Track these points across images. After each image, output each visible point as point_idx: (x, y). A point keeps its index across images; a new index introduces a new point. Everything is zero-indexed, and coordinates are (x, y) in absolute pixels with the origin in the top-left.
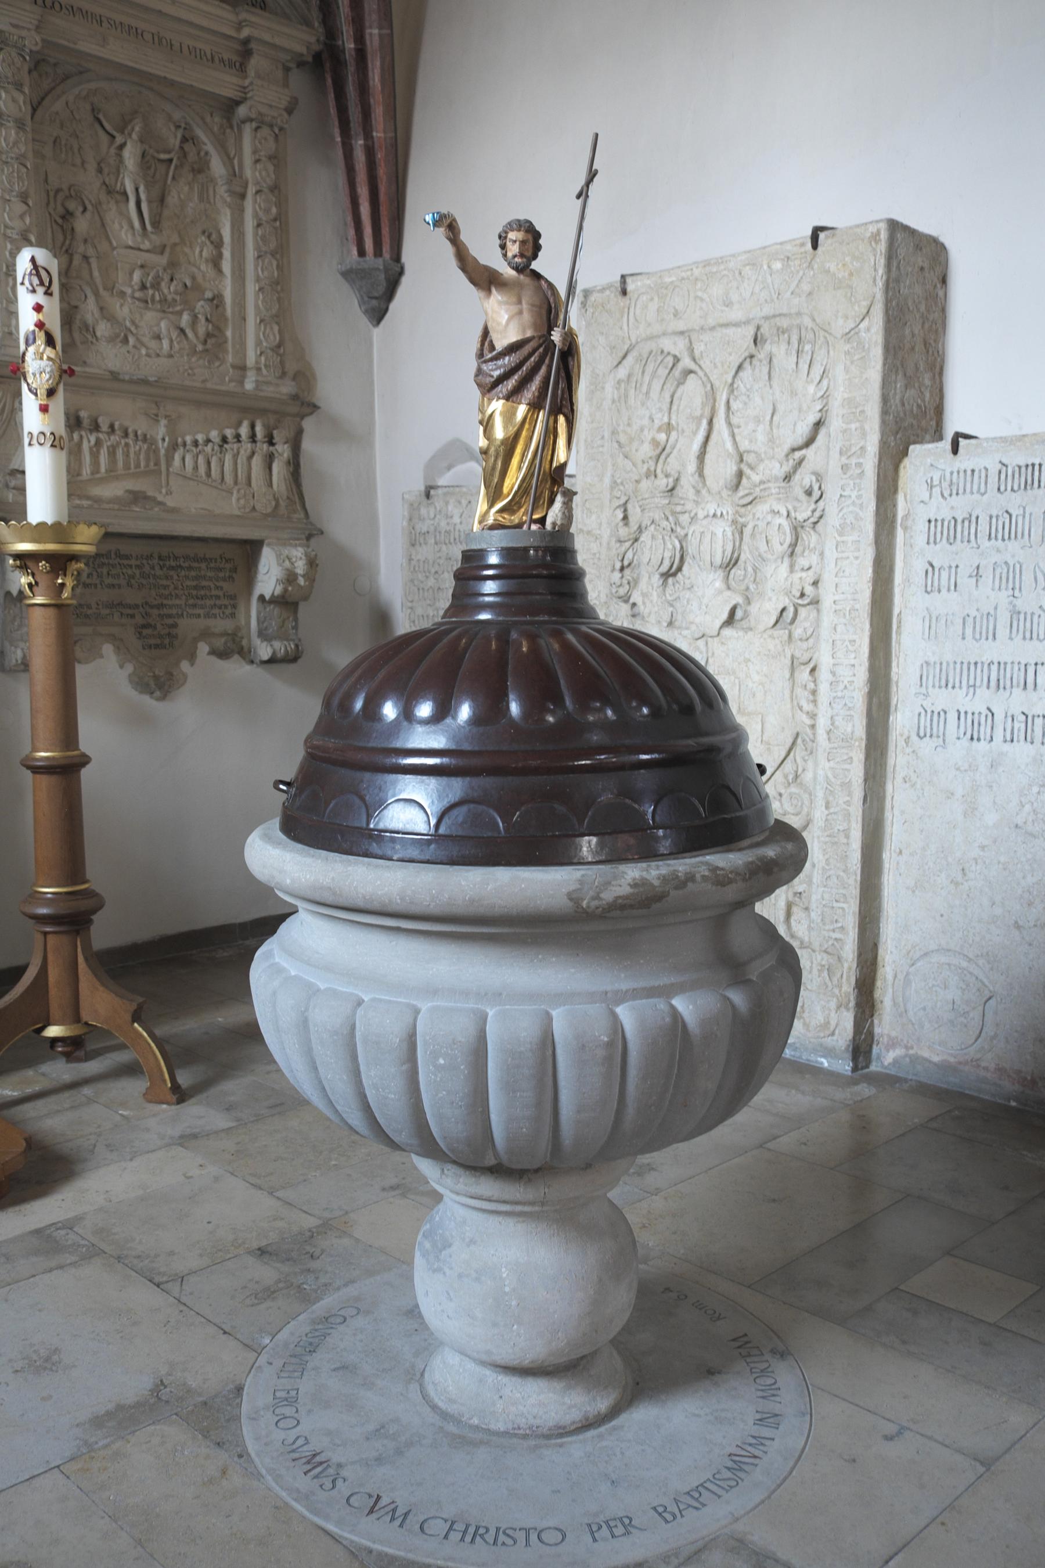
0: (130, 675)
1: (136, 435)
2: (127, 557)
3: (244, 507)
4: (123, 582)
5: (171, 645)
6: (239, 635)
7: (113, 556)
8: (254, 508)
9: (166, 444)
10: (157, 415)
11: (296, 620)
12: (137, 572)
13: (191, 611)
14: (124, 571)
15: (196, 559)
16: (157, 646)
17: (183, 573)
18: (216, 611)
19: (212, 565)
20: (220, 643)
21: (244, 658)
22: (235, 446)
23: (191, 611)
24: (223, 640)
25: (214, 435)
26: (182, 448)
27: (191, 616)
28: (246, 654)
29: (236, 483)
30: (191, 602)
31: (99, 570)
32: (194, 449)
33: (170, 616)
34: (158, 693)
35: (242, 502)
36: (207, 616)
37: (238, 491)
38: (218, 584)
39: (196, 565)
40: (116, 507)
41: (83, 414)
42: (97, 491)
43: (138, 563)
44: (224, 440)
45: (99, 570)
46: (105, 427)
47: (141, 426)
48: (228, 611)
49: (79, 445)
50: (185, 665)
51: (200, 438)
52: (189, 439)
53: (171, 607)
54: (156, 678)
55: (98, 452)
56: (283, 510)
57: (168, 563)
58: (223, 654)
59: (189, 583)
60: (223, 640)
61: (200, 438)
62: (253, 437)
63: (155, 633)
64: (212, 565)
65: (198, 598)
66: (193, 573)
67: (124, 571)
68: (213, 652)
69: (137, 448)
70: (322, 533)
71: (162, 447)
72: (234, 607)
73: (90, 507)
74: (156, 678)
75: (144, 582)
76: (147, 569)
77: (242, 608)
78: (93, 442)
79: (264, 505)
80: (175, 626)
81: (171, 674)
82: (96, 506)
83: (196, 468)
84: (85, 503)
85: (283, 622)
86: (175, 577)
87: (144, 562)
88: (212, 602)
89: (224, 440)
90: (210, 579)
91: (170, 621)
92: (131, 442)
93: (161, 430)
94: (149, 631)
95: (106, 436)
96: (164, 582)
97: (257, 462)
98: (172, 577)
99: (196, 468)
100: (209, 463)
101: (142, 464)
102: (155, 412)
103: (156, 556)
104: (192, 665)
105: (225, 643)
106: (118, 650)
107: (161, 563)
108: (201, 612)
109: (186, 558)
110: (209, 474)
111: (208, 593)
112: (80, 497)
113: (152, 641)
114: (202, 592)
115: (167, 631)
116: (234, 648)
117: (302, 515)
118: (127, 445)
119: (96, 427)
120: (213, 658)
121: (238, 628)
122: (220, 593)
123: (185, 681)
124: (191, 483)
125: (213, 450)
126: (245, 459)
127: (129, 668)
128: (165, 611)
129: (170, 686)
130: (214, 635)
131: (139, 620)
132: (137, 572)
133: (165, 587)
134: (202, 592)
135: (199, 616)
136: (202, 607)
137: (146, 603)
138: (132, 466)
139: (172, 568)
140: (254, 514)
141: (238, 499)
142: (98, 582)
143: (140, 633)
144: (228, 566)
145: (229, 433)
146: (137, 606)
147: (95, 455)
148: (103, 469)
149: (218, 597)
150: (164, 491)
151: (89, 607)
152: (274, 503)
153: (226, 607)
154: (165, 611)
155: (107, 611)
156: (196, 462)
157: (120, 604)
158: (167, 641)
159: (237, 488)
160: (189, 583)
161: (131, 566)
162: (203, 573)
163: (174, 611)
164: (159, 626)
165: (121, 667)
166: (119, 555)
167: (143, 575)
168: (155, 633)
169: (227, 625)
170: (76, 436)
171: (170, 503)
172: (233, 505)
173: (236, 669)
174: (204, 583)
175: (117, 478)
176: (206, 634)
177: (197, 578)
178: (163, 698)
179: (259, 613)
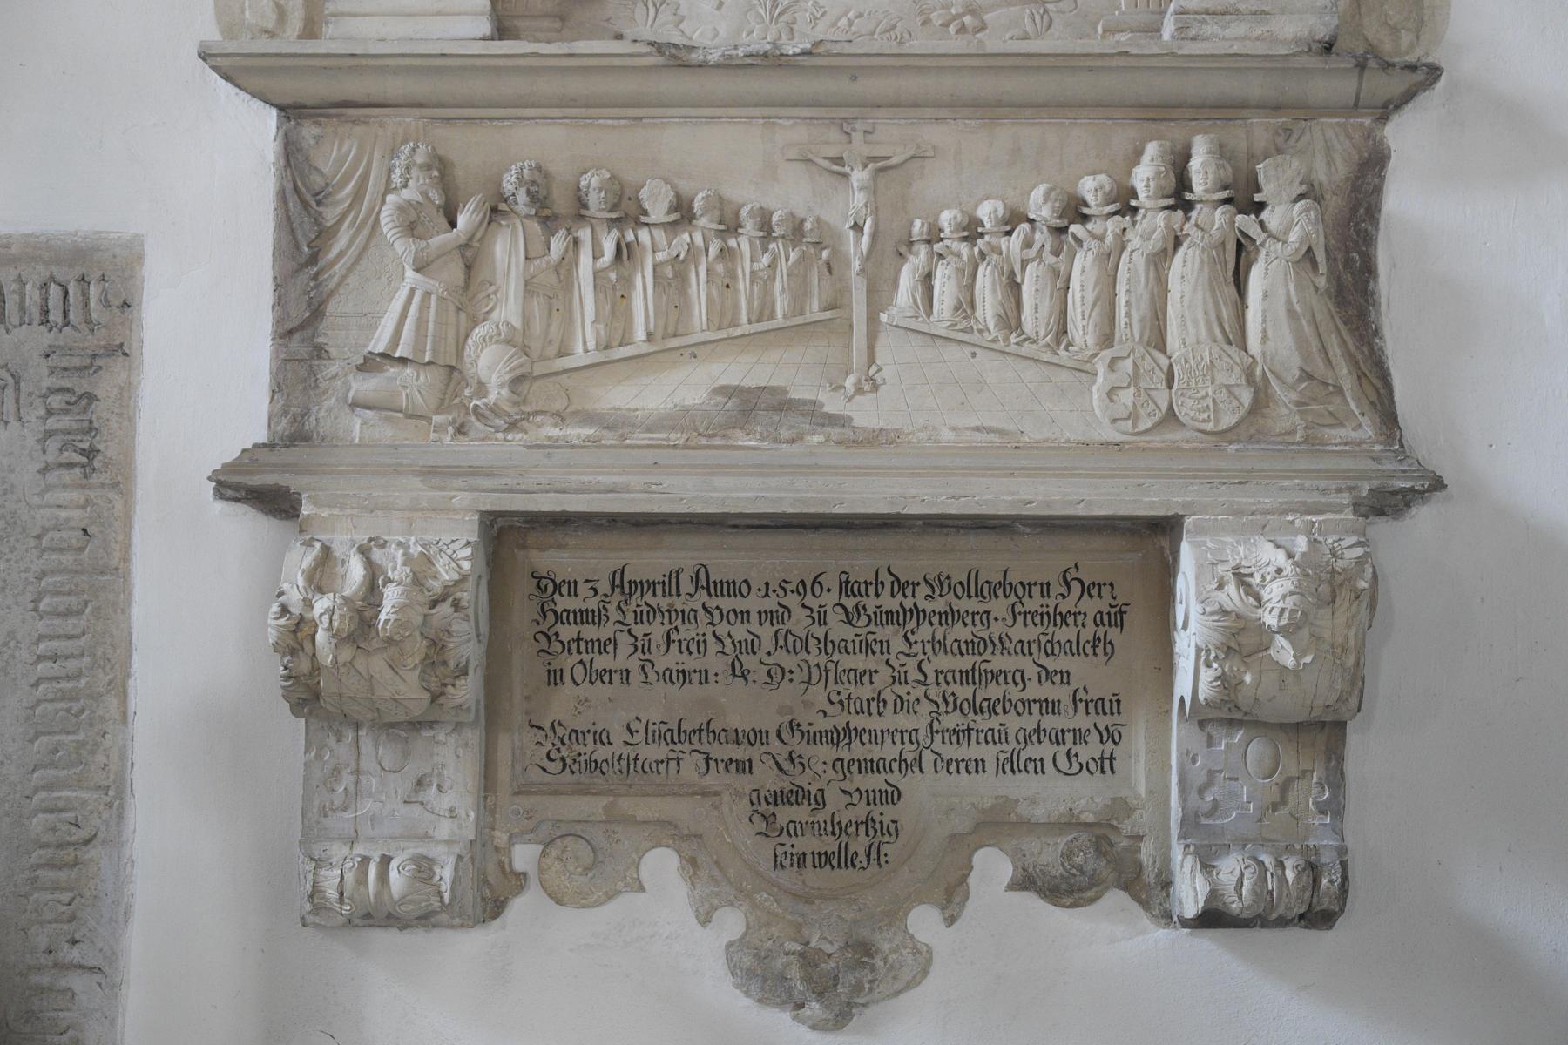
0: (730, 945)
1: (766, 226)
2: (733, 588)
3: (1134, 416)
4: (715, 662)
5: (875, 855)
6: (1126, 827)
7: (687, 586)
8: (1171, 416)
9: (866, 240)
10: (838, 160)
11: (1336, 779)
12: (766, 632)
13: (949, 751)
14: (722, 629)
15: (973, 586)
16: (823, 860)
17: (925, 632)
18: (1045, 750)
19: (1031, 605)
20: (1048, 854)
21: (1145, 905)
22: (1113, 225)
23: (949, 751)
24: (1063, 841)
25: (1040, 206)
26: (922, 250)
27: (949, 765)
28: (1150, 891)
29: (1107, 340)
30: (951, 721)
31: (638, 630)
32: (964, 248)
33: (873, 766)
34: (814, 1009)
35: (1126, 397)
36: (1010, 765)
37: (1112, 364)
38: (1051, 664)
39: (965, 604)
40: (677, 437)
41: (592, 181)
42: (619, 396)
43: (770, 604)
44: (1075, 211)
45: (638, 630)
46: (658, 212)
47: (792, 194)
48: (1086, 752)
49: (566, 268)
50: (924, 922)
51: (987, 212)
52: (946, 218)
53: (877, 737)
54: (809, 959)
55: (628, 282)
56: (1285, 413)
57: (871, 603)
58: (1065, 890)
59: (944, 662)
60: (1063, 841)
61: (987, 212)
62: (1179, 197)
63: (821, 817)
64: (1031, 605)
65: (978, 711)
66: (962, 632)
67: (722, 629)
68: (1025, 882)
69: (765, 260)
70: (1438, 484)
71: (856, 247)
72: (1112, 736)
73: (594, 442)
74: (809, 959)
75: (789, 661)
76: (799, 622)
77: (1137, 741)
78: (609, 248)
79: (1211, 400)
80: (892, 795)
81: (863, 951)
82: (609, 439)
83: (966, 305)
84: (576, 433)
85: (1285, 788)
86: (898, 645)
87: (792, 601)
88: (1029, 723)
89: (1075, 211)
90: (1025, 648)
91: (875, 782)
92: (745, 247)
93: (849, 204)
94: (801, 813)
95: (660, 234)
96: (860, 662)
97: (1185, 271)
98: (885, 646)
99: (966, 305)
100: (1014, 287)
101: (781, 305)
102: (832, 152)
103: (830, 580)
104: (951, 920)
105: (1068, 855)
106: (692, 864)
107: (850, 603)
108: (988, 752)
109: (939, 584)
110: (1011, 320)
111: (1014, 693)
112: (560, 418)
113: (809, 844)
114: (994, 691)
115: (861, 811)
116: (1098, 866)
117: (1368, 431)
118: (726, 253)
119: (625, 212)
120: (1031, 902)
121: (1123, 807)
122: (1062, 693)
123: (925, 972)
124: (952, 352)
125: (1028, 244)
126: (1140, 261)
127: (731, 923)
128: (858, 751)
129: (858, 988)
130: (1028, 826)
131: (767, 778)
132: (766, 632)
133: (858, 677)
134: (994, 691)
135: (980, 765)
136: (993, 737)
137: (793, 726)
138: (744, 319)
139: (890, 617)
140: (1172, 435)
141: (1111, 393)
142: (633, 665)
143: (768, 819)
144: (1090, 606)
145: (1090, 187)
146: (759, 736)
147: (614, 295)
148: (640, 334)
149: (1052, 707)
150: (850, 382)
151: (602, 738)
152: (1246, 397)
153: (1080, 736)
154: (858, 751)
155: (662, 752)
156: (971, 287)
157: (705, 729)
158: (860, 844)
159: (1107, 354)
160: (944, 662)
161: (745, 616)
162: (996, 629)
163: (890, 751)
164: (834, 798)
165: (705, 920)
166: (705, 582)
167: (784, 641)
168: (821, 817)
169: (1086, 795)
170: (558, 244)
171: (866, 414)
172: (1093, 410)
173: (1111, 935)
174: (999, 662)
175: (693, 352)
176: (996, 825)
177: (974, 646)
178: (840, 1019)
179: (1189, 757)
